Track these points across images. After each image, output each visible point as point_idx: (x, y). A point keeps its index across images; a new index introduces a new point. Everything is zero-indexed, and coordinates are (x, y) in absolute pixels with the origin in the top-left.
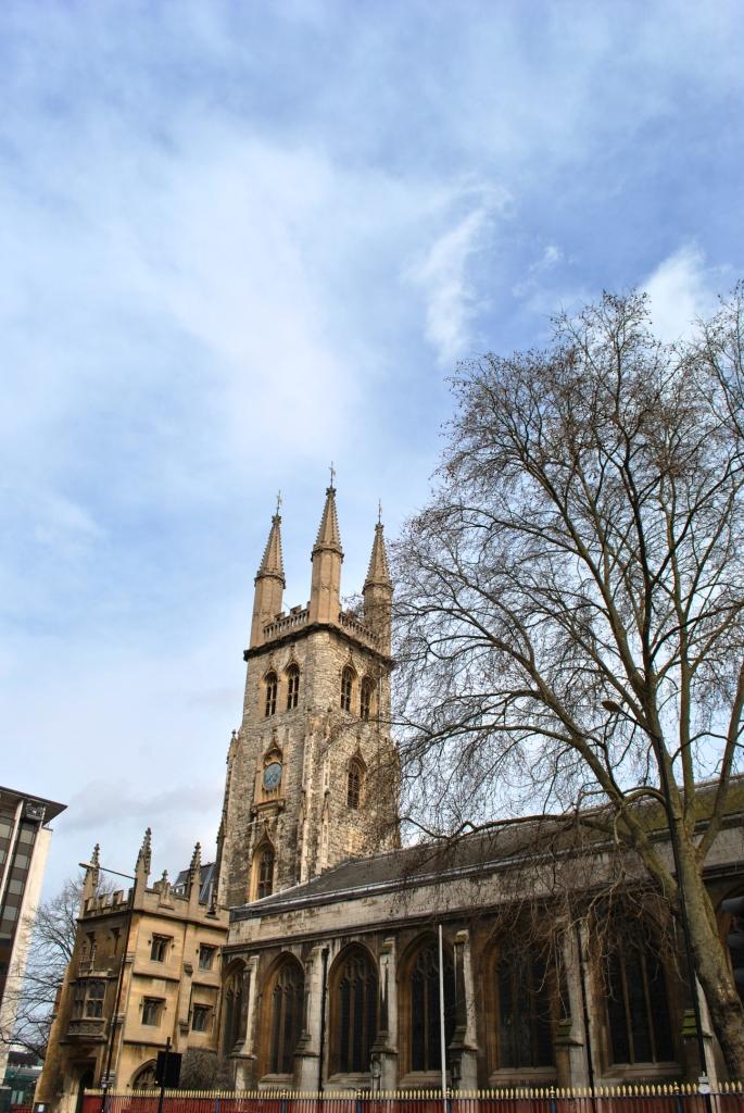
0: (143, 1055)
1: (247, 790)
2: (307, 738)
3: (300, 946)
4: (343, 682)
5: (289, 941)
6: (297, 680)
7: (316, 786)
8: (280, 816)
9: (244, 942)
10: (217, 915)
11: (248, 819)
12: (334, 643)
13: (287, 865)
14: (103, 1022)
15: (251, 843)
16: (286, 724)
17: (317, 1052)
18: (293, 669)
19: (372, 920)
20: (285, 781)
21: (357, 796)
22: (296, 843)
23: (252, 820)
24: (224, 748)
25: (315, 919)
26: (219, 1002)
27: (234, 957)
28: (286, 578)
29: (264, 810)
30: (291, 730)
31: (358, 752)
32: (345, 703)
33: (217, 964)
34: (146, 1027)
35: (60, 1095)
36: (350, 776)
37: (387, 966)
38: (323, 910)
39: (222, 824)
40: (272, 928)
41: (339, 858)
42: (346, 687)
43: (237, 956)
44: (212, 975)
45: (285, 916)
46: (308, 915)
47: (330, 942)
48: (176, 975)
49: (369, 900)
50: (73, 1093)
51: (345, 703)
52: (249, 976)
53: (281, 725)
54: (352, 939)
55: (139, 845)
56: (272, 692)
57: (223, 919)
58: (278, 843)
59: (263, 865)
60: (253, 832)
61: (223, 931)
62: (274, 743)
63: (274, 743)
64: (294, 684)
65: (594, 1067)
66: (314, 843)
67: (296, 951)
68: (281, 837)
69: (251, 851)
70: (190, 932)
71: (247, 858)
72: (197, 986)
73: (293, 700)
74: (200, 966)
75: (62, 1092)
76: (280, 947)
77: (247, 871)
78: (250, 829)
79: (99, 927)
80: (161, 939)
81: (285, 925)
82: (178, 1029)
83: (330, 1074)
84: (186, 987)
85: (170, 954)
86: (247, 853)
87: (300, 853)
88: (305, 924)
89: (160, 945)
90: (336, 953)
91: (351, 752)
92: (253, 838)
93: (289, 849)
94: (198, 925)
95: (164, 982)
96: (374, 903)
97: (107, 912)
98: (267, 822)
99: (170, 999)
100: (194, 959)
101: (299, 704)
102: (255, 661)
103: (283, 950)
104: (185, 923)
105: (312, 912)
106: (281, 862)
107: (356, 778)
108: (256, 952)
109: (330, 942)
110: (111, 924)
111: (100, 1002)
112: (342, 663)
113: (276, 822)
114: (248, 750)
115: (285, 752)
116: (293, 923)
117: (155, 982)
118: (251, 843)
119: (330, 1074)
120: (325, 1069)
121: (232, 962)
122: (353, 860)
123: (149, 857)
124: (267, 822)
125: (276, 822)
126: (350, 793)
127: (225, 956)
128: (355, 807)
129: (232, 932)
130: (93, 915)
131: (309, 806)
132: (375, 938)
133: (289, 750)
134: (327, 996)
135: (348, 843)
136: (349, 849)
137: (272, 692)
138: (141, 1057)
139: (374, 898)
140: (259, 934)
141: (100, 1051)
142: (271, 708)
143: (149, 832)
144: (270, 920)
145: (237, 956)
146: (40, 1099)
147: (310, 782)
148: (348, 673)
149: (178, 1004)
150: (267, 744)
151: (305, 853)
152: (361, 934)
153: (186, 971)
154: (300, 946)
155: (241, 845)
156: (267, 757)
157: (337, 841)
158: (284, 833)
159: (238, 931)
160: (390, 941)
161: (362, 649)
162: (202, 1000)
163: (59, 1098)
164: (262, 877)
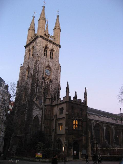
20: (52, 76)
63: (49, 65)
68: (51, 88)
78: (42, 82)
96: (100, 117)
124: (48, 83)
130: (73, 102)
133: (53, 69)
150: (47, 64)
156: (47, 67)
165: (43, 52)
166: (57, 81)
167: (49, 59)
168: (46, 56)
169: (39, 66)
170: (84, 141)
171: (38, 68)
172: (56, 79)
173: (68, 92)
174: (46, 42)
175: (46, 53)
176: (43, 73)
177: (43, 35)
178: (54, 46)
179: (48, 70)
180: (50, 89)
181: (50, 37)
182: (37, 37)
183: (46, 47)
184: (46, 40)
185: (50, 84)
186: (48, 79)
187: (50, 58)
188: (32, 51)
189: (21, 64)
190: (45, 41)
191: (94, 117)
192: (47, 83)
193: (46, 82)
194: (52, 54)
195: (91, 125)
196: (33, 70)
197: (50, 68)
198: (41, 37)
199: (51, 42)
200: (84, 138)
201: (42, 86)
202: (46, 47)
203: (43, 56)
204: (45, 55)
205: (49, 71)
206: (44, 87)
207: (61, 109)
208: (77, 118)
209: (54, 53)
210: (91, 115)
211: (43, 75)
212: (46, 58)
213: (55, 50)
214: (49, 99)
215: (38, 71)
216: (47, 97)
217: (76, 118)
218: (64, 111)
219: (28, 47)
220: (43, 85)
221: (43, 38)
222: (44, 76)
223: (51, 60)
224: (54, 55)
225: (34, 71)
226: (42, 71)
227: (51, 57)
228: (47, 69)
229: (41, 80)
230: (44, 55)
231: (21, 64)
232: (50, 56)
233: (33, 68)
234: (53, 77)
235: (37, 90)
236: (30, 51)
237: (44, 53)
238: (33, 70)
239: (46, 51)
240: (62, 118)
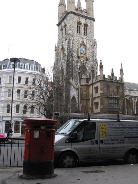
11: (77, 58)
20: (88, 53)
30: (88, 41)
63: (83, 42)
68: (88, 67)
78: (78, 61)
110: (115, 84)
124: (83, 61)
130: (107, 80)
133: (88, 46)
150: (81, 41)
156: (81, 44)
158: (88, 66)
165: (76, 30)
166: (94, 58)
167: (83, 36)
168: (80, 33)
169: (72, 45)
171: (72, 47)
172: (92, 56)
173: (101, 70)
174: (78, 17)
175: (79, 30)
176: (78, 51)
177: (74, 11)
178: (87, 20)
179: (83, 48)
180: (87, 68)
181: (82, 11)
182: (68, 13)
183: (79, 24)
184: (76, 15)
185: (86, 63)
187: (84, 34)
188: (64, 29)
189: (55, 45)
190: (77, 17)
191: (135, 93)
192: (82, 62)
193: (82, 61)
194: (85, 29)
195: (131, 102)
196: (67, 50)
197: (85, 45)
198: (72, 12)
199: (83, 16)
201: (78, 65)
202: (79, 24)
203: (76, 33)
204: (79, 31)
205: (83, 49)
206: (80, 66)
207: (96, 88)
208: (113, 96)
209: (88, 28)
210: (132, 91)
211: (78, 54)
212: (80, 36)
213: (89, 25)
214: (85, 78)
215: (72, 51)
216: (82, 77)
217: (111, 96)
218: (99, 90)
219: (60, 26)
220: (79, 65)
221: (74, 13)
222: (79, 55)
223: (85, 37)
224: (88, 30)
225: (67, 51)
226: (77, 50)
227: (85, 33)
229: (75, 59)
230: (77, 32)
231: (55, 45)
232: (84, 32)
233: (67, 48)
235: (72, 70)
236: (62, 29)
237: (77, 30)
238: (66, 50)
239: (78, 27)
240: (97, 97)
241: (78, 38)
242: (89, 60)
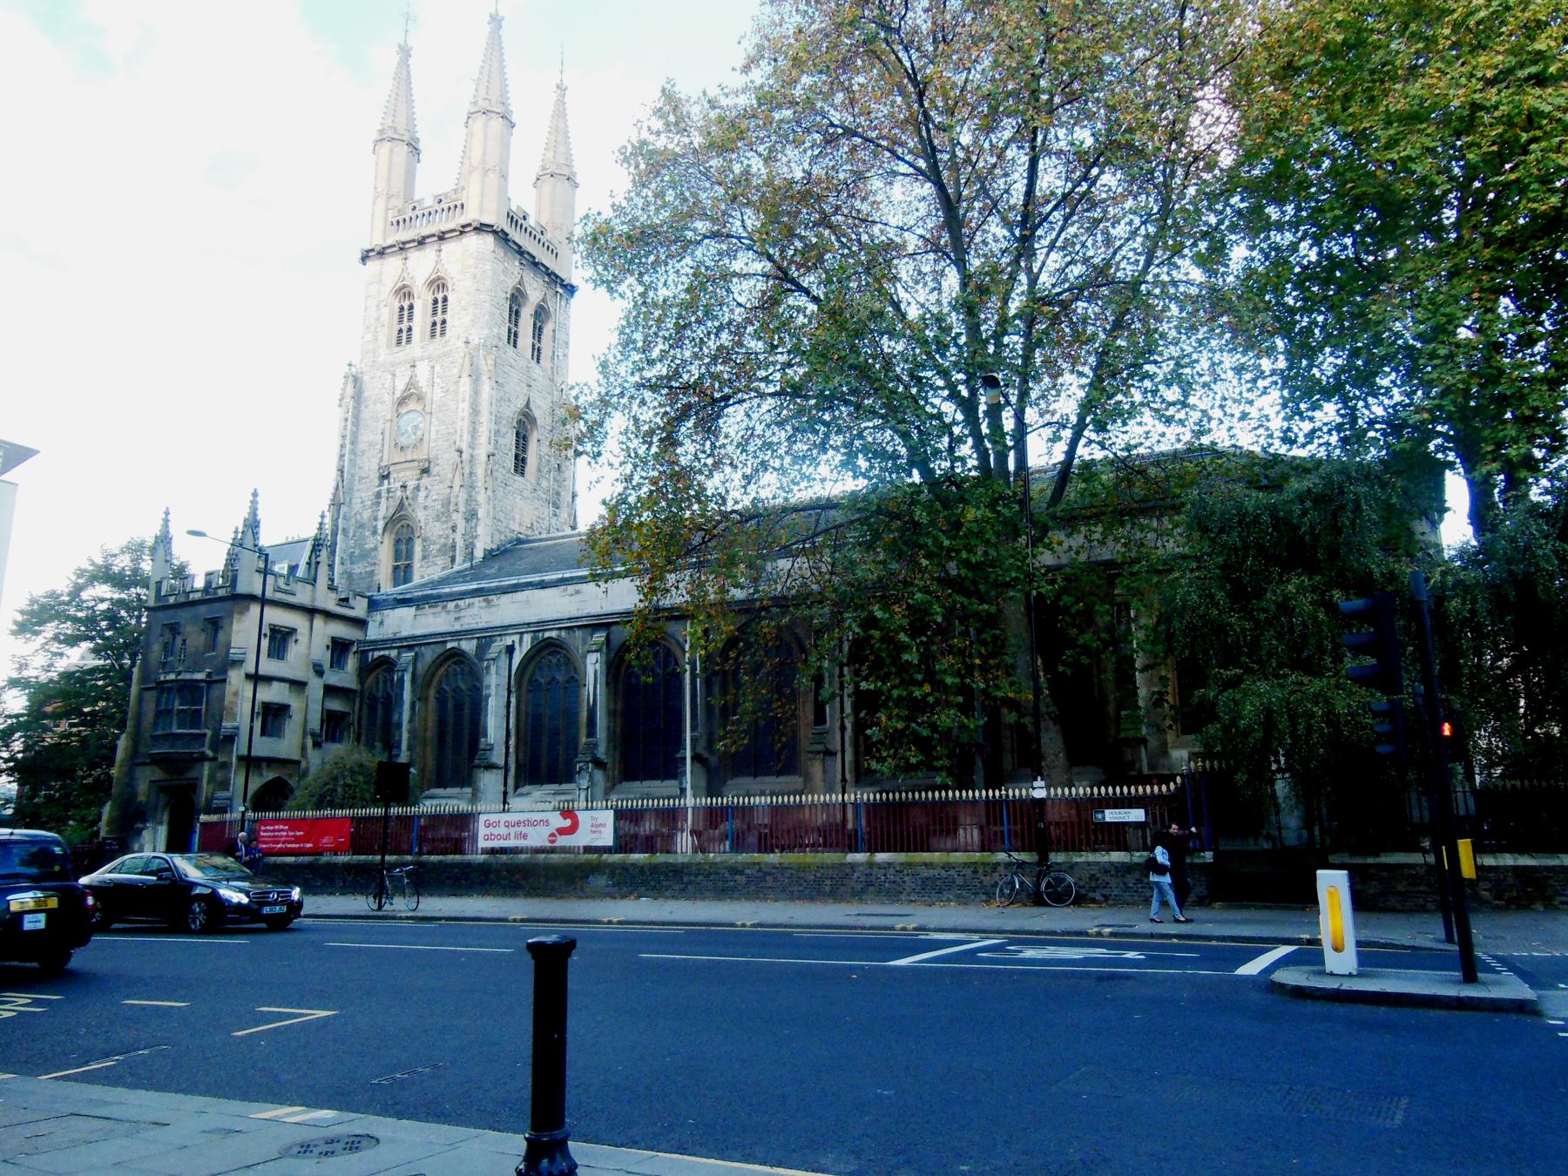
0: (265, 773)
1: (371, 444)
2: (463, 380)
3: (475, 642)
4: (511, 310)
5: (456, 635)
6: (445, 299)
7: (472, 446)
8: (423, 481)
9: (391, 636)
10: (352, 602)
11: (377, 482)
12: (500, 252)
13: (435, 543)
14: (205, 735)
15: (381, 514)
16: (430, 358)
17: (501, 762)
18: (438, 284)
19: (575, 614)
21: (524, 460)
22: (449, 516)
23: (381, 484)
24: (336, 385)
25: (492, 610)
26: (357, 709)
27: (377, 654)
28: (421, 146)
29: (398, 472)
30: (437, 368)
31: (527, 405)
32: (513, 337)
33: (352, 663)
34: (264, 738)
35: (140, 825)
36: (518, 434)
37: (593, 666)
38: (506, 598)
39: (337, 488)
40: (431, 619)
41: (503, 537)
42: (515, 315)
43: (382, 653)
44: (347, 676)
45: (451, 605)
46: (484, 604)
47: (517, 637)
48: (298, 675)
49: (571, 589)
50: (161, 823)
51: (513, 337)
52: (403, 677)
53: (422, 359)
54: (547, 634)
55: (244, 512)
56: (406, 313)
57: (359, 609)
58: (420, 515)
59: (398, 542)
60: (383, 500)
61: (361, 623)
62: (411, 383)
63: (411, 383)
64: (440, 305)
65: (848, 776)
66: (472, 516)
67: (468, 646)
68: (426, 508)
69: (380, 525)
70: (318, 622)
71: (375, 533)
72: (330, 691)
73: (438, 328)
74: (332, 666)
75: (144, 821)
76: (445, 642)
77: (375, 549)
78: (378, 495)
79: (183, 616)
80: (279, 632)
81: (453, 616)
82: (309, 742)
83: (516, 787)
84: (316, 687)
85: (295, 651)
86: (375, 527)
87: (454, 529)
88: (477, 615)
89: (280, 639)
90: (525, 651)
91: (520, 404)
92: (383, 506)
93: (437, 524)
94: (329, 615)
95: (287, 685)
96: (577, 592)
97: (197, 596)
98: (404, 487)
99: (295, 704)
100: (325, 657)
101: (448, 333)
102: (374, 265)
103: (449, 645)
104: (311, 612)
105: (488, 602)
106: (424, 540)
107: (525, 438)
108: (410, 648)
109: (517, 637)
110: (203, 610)
111: (199, 711)
112: (511, 283)
113: (417, 488)
114: (370, 391)
115: (428, 397)
116: (463, 613)
117: (275, 684)
118: (381, 514)
119: (516, 787)
120: (511, 781)
121: (373, 660)
122: (520, 541)
123: (257, 527)
124: (404, 487)
125: (417, 488)
126: (517, 456)
127: (363, 654)
128: (523, 474)
129: (371, 625)
130: (172, 600)
131: (467, 471)
132: (579, 633)
134: (513, 700)
135: (514, 519)
136: (516, 527)
137: (406, 313)
138: (261, 775)
139: (578, 587)
140: (413, 627)
141: (201, 772)
142: (404, 336)
143: (255, 494)
144: (427, 610)
145: (382, 653)
146: (108, 833)
147: (466, 437)
148: (516, 298)
149: (308, 709)
150: (400, 385)
151: (461, 529)
152: (560, 629)
153: (316, 672)
154: (475, 642)
155: (367, 515)
156: (402, 401)
157: (501, 516)
158: (429, 503)
159: (381, 623)
160: (600, 637)
161: (535, 264)
162: (336, 705)
163: (139, 832)
164: (397, 555)
170: (209, 782)
179: (416, 415)
186: (407, 465)
192: (399, 493)
197: (420, 398)
200: (206, 772)
211: (381, 458)
228: (403, 410)
234: (436, 440)
241: (390, 376)
242: (434, 470)
